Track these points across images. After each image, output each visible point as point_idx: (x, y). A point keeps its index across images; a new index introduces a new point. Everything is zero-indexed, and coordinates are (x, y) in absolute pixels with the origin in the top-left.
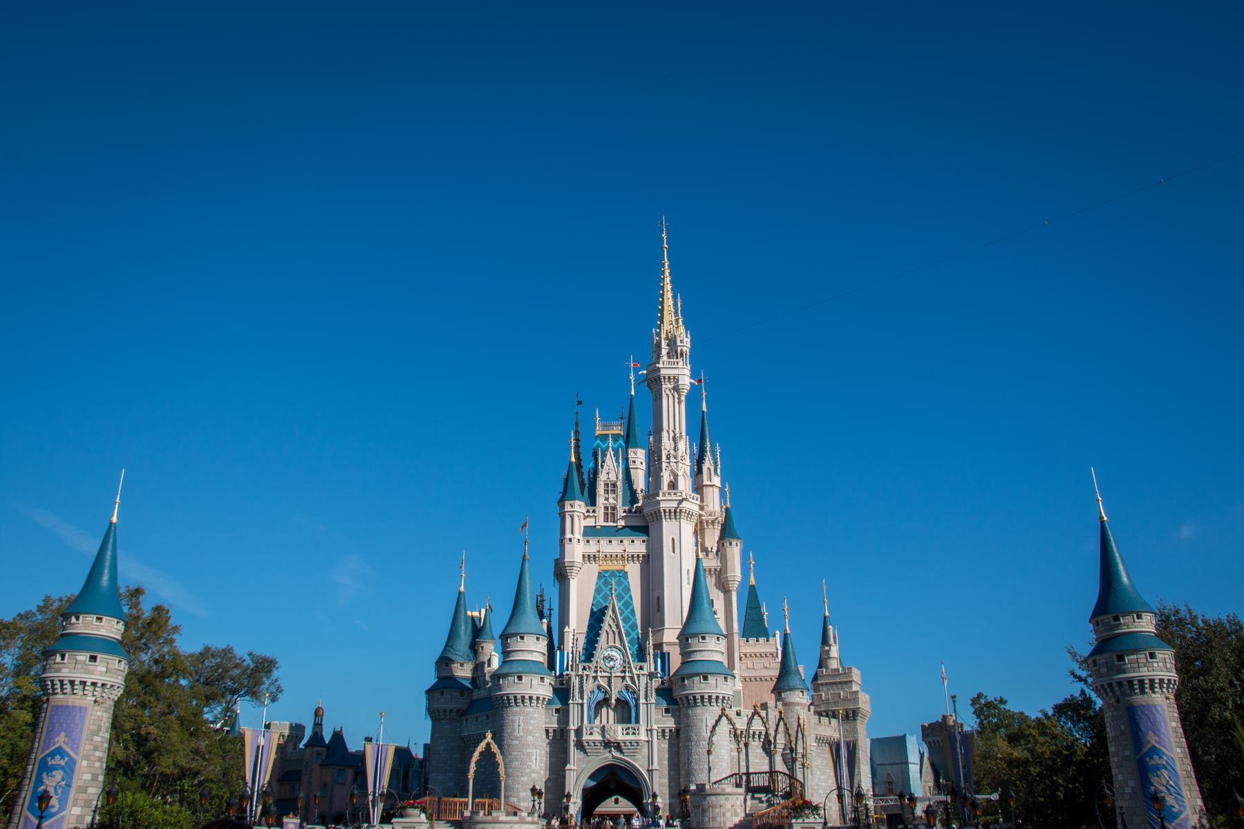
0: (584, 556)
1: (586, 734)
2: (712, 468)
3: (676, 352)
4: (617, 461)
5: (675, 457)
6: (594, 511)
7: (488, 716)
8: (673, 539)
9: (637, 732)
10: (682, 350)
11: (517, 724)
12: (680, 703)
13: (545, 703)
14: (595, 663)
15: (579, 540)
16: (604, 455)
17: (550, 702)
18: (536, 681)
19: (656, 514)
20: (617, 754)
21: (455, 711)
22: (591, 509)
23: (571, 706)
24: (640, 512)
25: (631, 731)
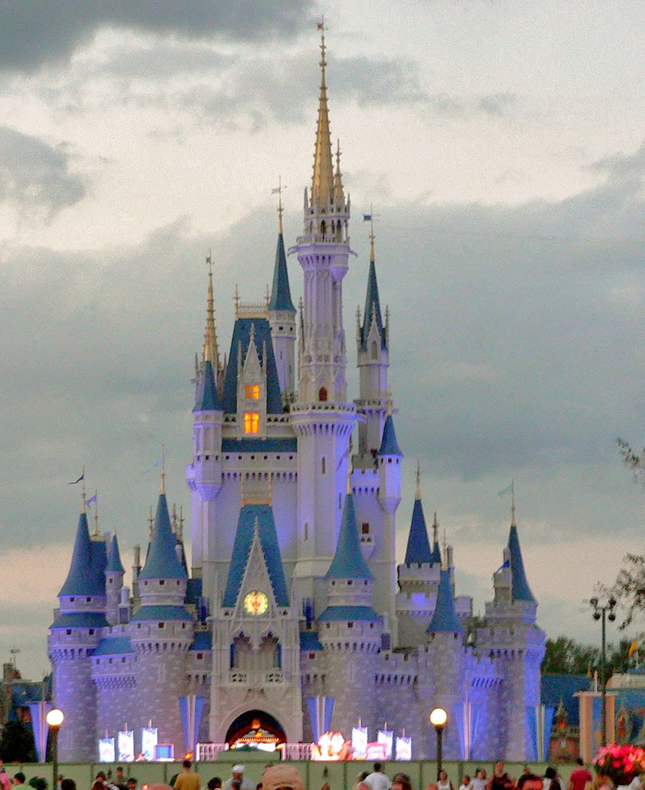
0: (223, 474)
2: (379, 343)
3: (333, 222)
4: (260, 358)
5: (327, 359)
6: (234, 420)
7: (124, 660)
8: (324, 459)
10: (339, 222)
11: (159, 672)
14: (236, 607)
15: (217, 457)
16: (245, 351)
17: (191, 647)
18: (179, 628)
19: (305, 429)
20: (261, 700)
21: (85, 650)
22: (231, 416)
23: (214, 653)
24: (288, 420)
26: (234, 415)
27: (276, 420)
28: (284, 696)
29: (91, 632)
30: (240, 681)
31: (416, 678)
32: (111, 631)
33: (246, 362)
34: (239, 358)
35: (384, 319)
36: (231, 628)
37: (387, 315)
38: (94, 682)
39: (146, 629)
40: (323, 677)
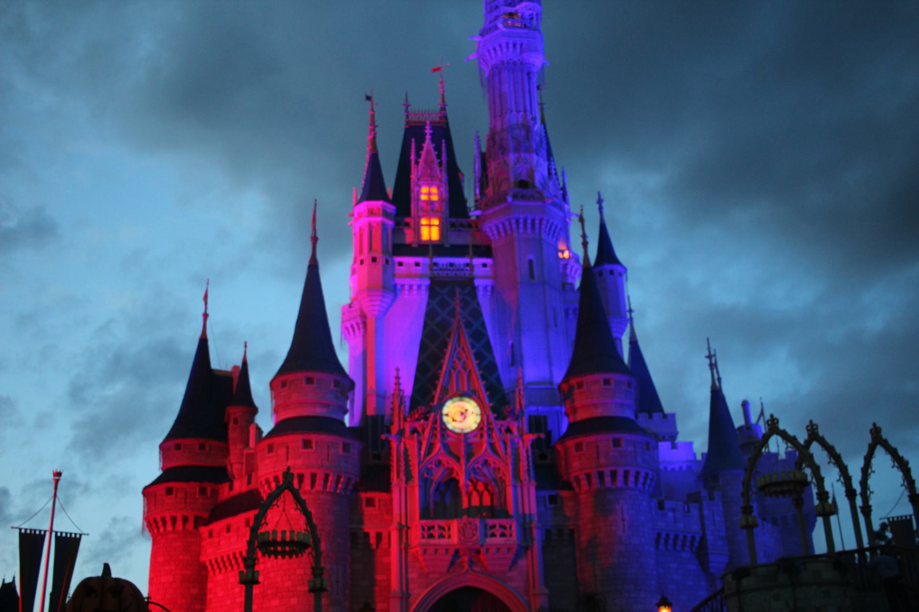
1: (424, 537)
4: (439, 156)
8: (530, 262)
9: (507, 532)
12: (575, 485)
13: (350, 487)
16: (419, 148)
24: (476, 227)
25: (498, 531)
26: (407, 220)
27: (462, 225)
28: (514, 562)
29: (203, 491)
30: (441, 536)
31: (703, 539)
32: (231, 488)
33: (421, 160)
34: (413, 157)
35: (561, 179)
36: (422, 452)
37: (563, 175)
38: (203, 567)
39: (283, 451)
40: (572, 532)
